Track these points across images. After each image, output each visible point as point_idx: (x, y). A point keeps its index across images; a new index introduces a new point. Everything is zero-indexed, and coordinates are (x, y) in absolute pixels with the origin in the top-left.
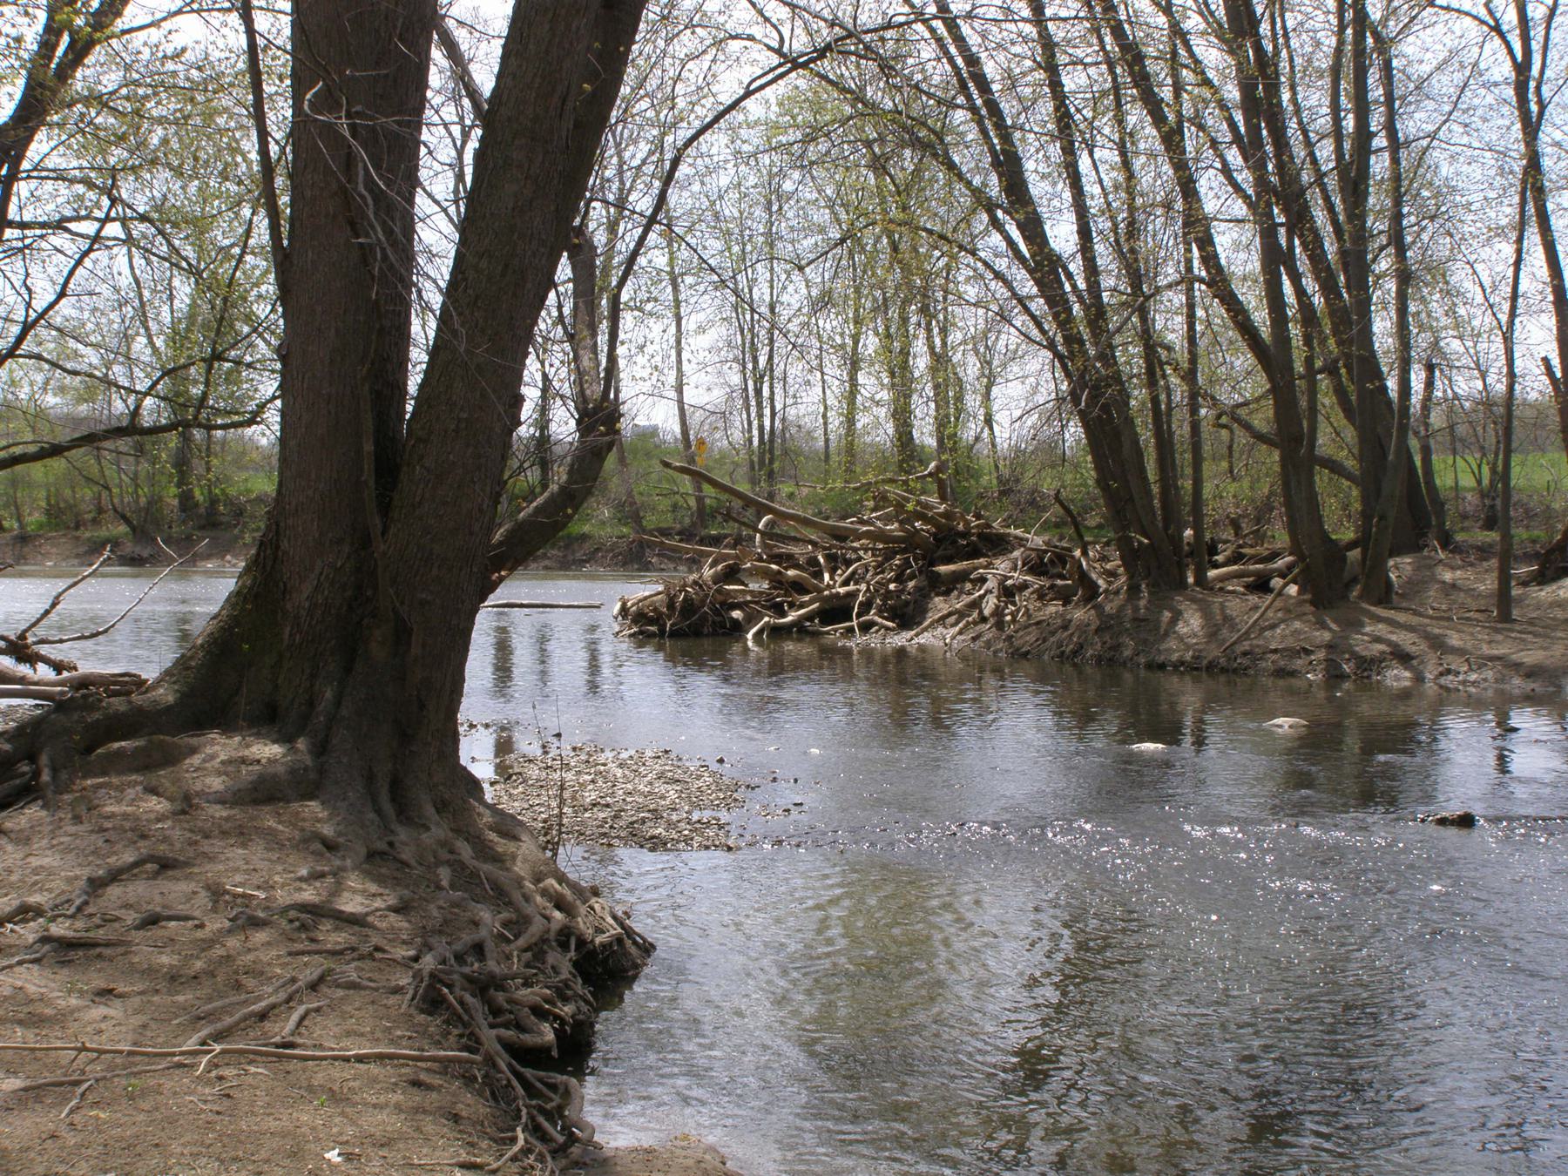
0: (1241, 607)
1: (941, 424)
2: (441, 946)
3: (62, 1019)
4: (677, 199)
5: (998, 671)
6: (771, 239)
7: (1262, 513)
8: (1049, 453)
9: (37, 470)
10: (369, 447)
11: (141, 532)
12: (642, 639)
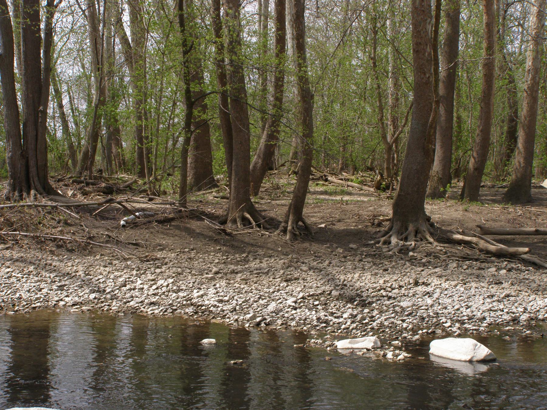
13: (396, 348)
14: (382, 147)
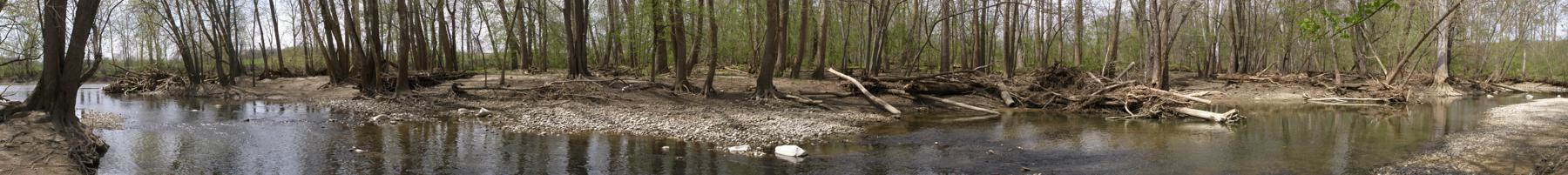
0: (210, 86)
1: (158, 56)
2: (73, 147)
3: (9, 159)
4: (111, 18)
5: (168, 98)
6: (127, 25)
7: (213, 71)
8: (176, 61)
9: (2, 67)
10: (59, 62)
11: (20, 78)
12: (106, 94)
13: (759, 150)
14: (752, 52)
